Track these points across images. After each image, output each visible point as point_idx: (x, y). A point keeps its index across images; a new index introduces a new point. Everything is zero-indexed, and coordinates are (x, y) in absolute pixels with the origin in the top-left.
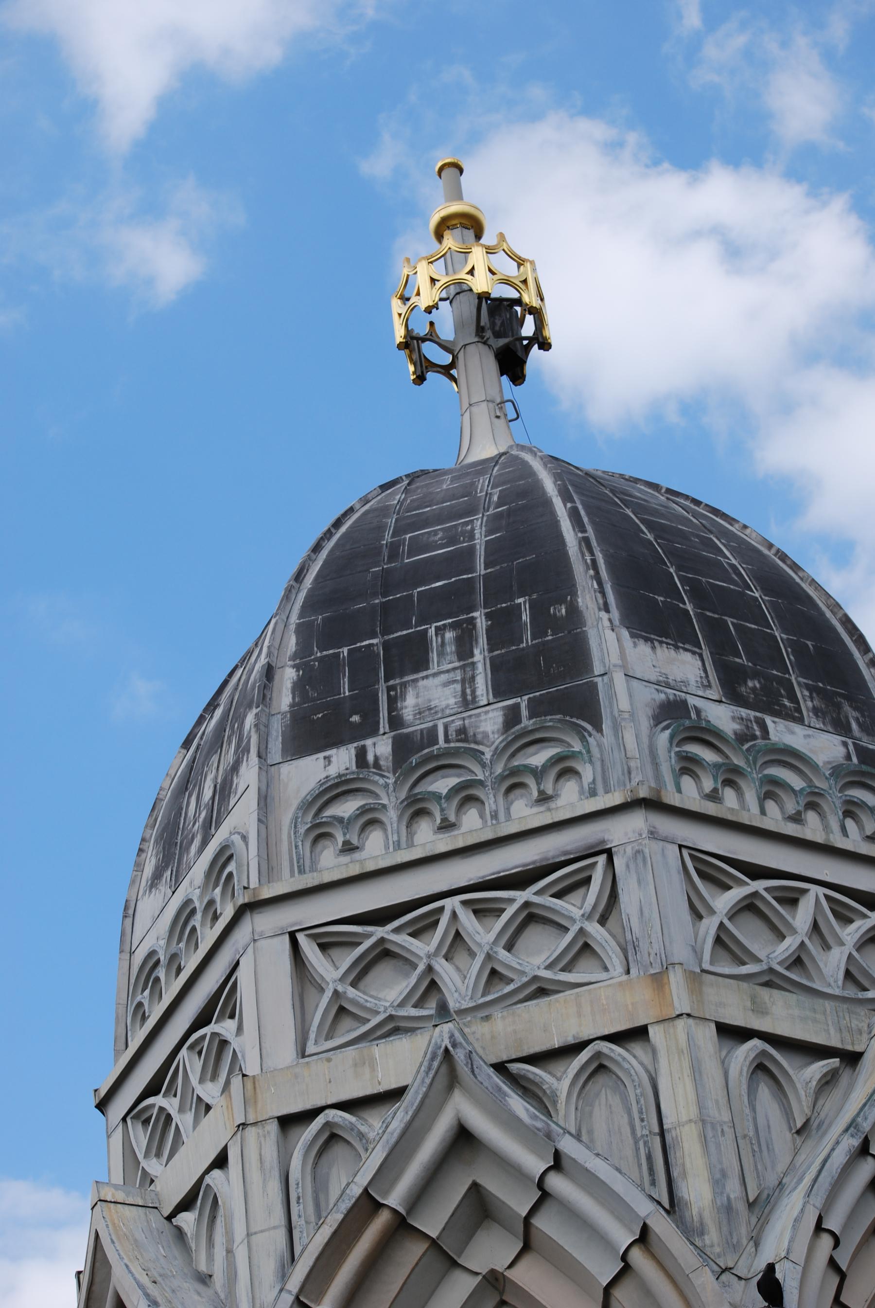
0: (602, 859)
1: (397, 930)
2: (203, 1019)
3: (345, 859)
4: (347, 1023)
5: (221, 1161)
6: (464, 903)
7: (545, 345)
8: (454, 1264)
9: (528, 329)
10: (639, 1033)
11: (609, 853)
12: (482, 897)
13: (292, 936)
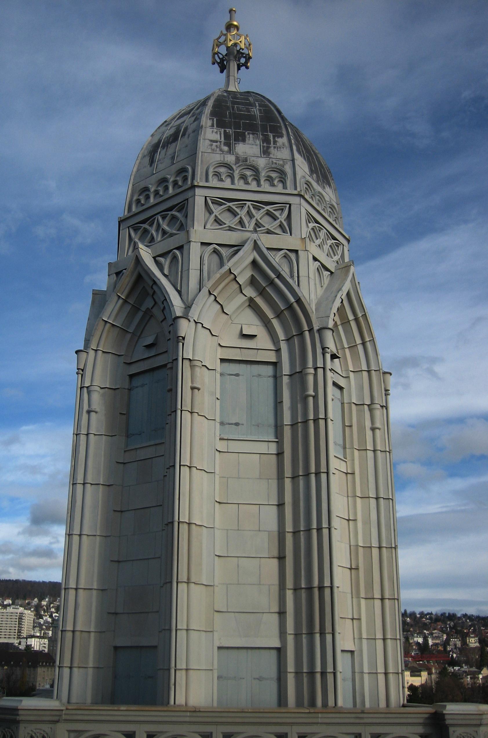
0: (288, 206)
1: (233, 205)
2: (170, 209)
3: (220, 183)
4: (216, 224)
5: (180, 248)
6: (251, 204)
7: (247, 68)
8: (242, 292)
9: (243, 60)
10: (296, 252)
11: (290, 205)
12: (258, 205)
13: (206, 197)
